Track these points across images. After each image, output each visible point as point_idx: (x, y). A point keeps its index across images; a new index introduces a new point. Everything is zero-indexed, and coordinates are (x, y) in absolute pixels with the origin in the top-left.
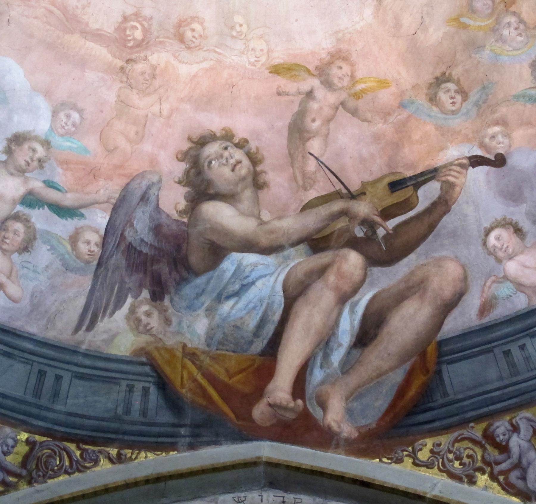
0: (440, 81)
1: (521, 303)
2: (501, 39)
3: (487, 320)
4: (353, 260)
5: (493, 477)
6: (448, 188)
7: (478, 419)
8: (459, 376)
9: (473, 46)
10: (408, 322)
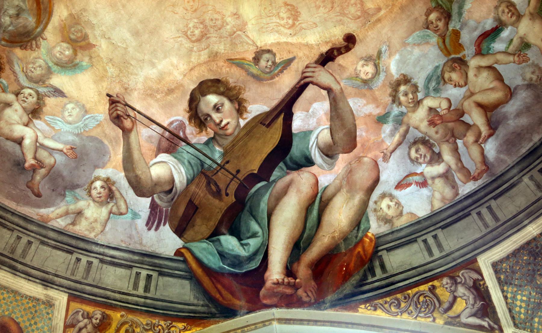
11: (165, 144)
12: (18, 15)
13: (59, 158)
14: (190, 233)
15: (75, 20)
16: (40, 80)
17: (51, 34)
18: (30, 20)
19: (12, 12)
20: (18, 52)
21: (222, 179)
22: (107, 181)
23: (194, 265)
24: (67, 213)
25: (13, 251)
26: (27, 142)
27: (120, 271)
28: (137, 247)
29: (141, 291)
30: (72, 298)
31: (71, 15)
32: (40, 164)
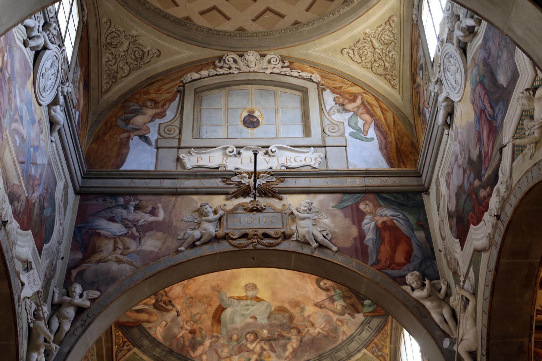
0: (192, 298)
1: (152, 333)
2: (202, 305)
3: (147, 330)
4: (153, 301)
5: (117, 348)
6: (172, 310)
7: (127, 338)
8: (135, 331)
9: (200, 301)
10: (143, 316)
11: (331, 301)
12: (284, 317)
13: (327, 326)
14: (360, 310)
15: (290, 302)
16: (304, 319)
17: (292, 311)
18: (287, 315)
19: (283, 319)
20: (295, 321)
21: (346, 293)
22: (338, 320)
23: (370, 314)
24: (343, 334)
25: (347, 352)
26: (320, 331)
27: (364, 333)
28: (359, 325)
29: (372, 331)
30: (366, 348)
31: (288, 303)
32: (327, 332)
